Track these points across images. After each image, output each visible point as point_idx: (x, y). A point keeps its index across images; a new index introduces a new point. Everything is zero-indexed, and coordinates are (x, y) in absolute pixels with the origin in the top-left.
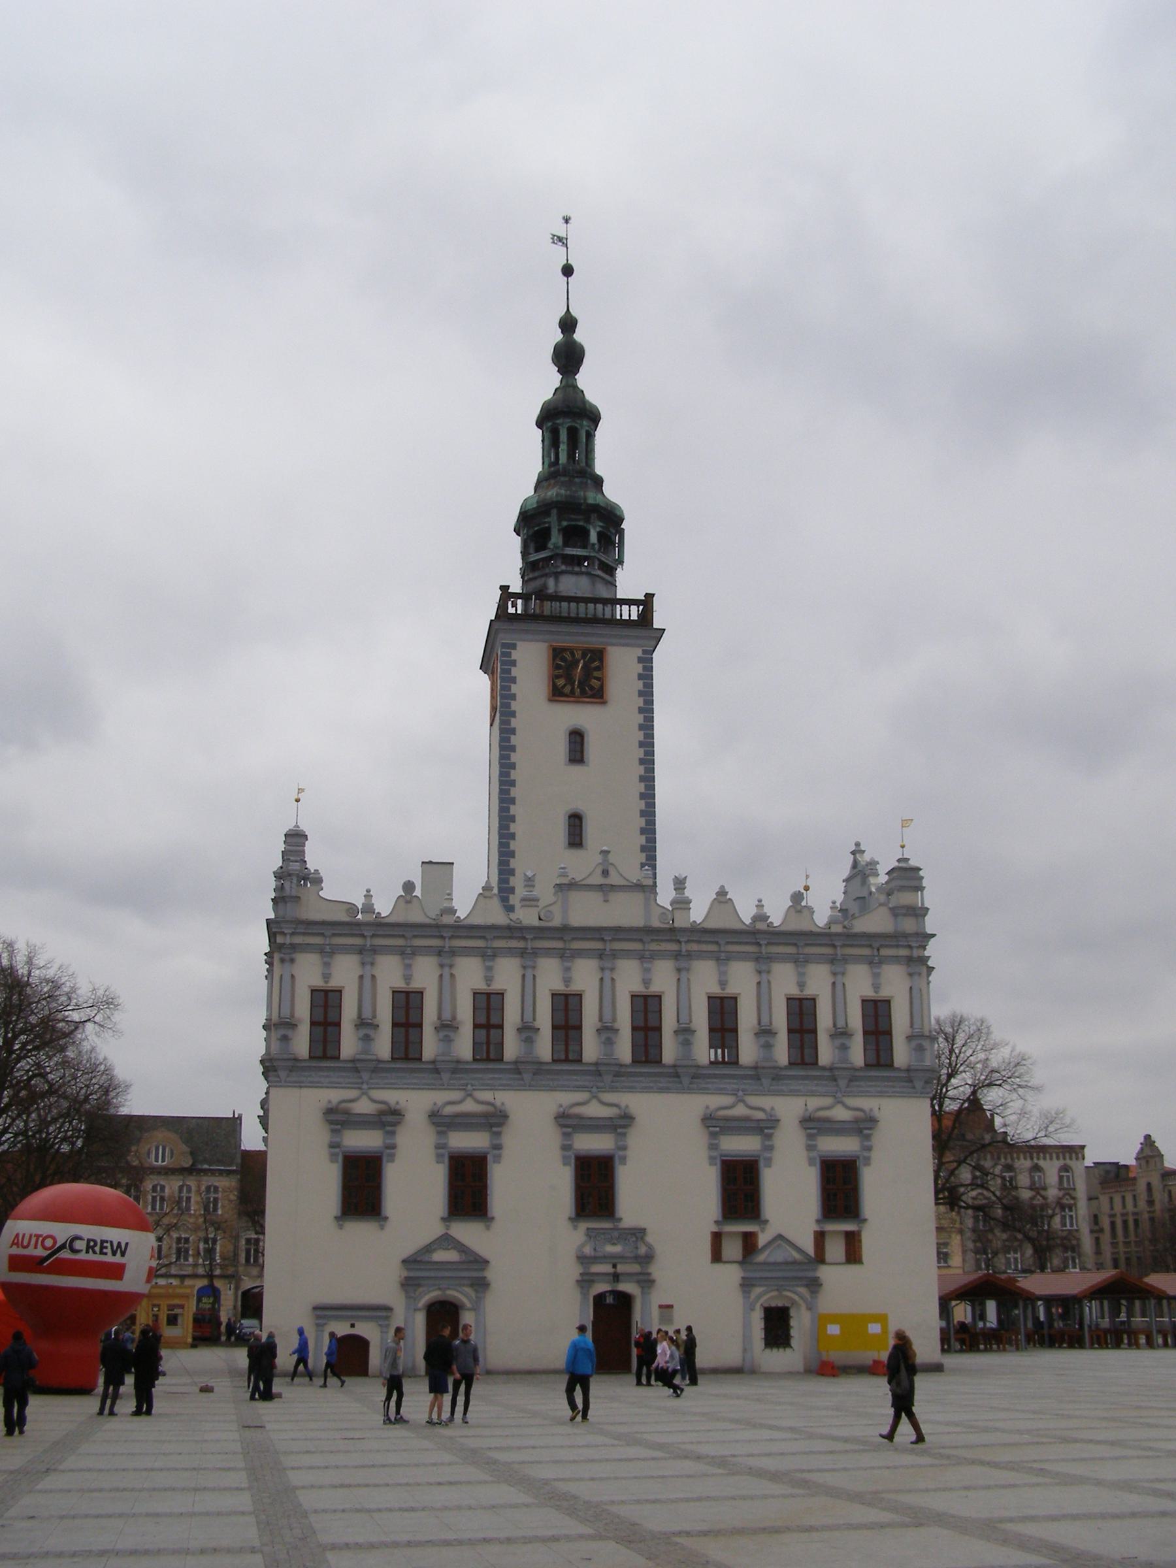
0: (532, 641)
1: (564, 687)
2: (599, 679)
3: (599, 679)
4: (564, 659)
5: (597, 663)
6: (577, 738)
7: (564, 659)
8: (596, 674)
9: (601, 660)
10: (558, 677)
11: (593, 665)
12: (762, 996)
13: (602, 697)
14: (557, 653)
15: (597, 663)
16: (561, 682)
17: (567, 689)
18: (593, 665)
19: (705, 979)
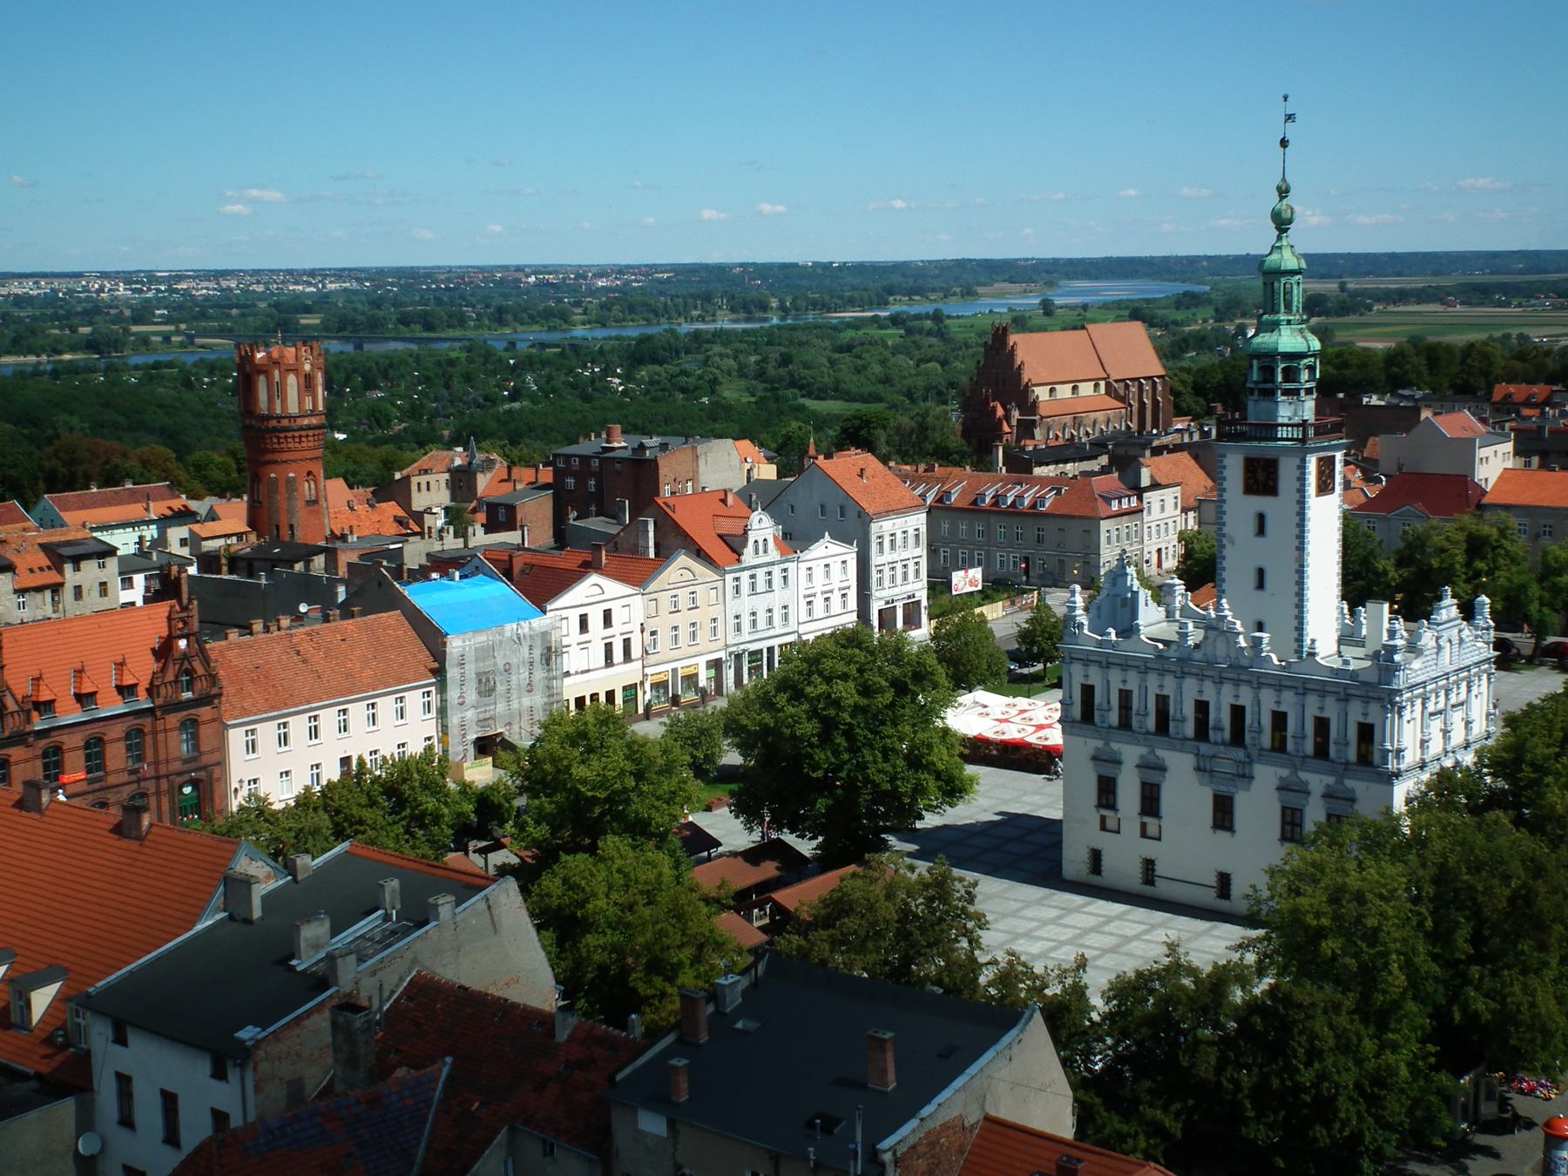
6: (1261, 518)
12: (1302, 716)
19: (1268, 700)
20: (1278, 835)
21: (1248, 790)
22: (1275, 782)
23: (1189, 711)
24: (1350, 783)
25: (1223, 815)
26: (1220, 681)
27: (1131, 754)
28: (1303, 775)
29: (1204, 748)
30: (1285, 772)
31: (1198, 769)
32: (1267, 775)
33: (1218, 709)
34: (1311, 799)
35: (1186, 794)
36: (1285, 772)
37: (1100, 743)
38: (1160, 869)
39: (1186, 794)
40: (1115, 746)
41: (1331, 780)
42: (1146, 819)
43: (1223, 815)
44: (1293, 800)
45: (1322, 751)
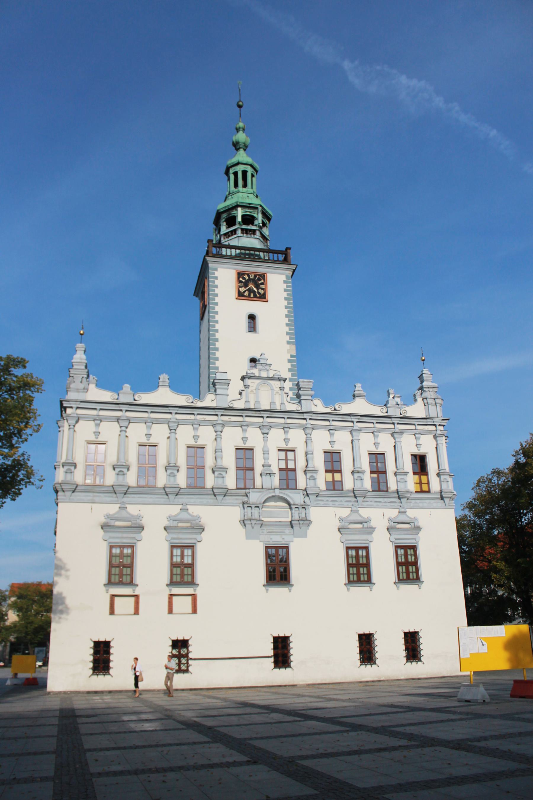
0: (227, 268)
1: (244, 292)
2: (263, 289)
3: (263, 289)
4: (244, 278)
5: (262, 281)
7: (244, 278)
8: (262, 286)
9: (264, 280)
10: (240, 287)
11: (260, 282)
13: (265, 298)
14: (240, 275)
15: (262, 281)
16: (242, 290)
17: (246, 294)
18: (260, 282)
20: (344, 579)
21: (305, 536)
22: (338, 524)
23: (229, 460)
24: (411, 513)
25: (278, 572)
26: (265, 430)
27: (155, 516)
28: (365, 513)
29: (254, 497)
30: (345, 512)
31: (243, 522)
32: (325, 518)
33: (266, 452)
34: (375, 535)
35: (229, 552)
36: (345, 512)
37: (113, 509)
38: (194, 651)
39: (229, 552)
40: (133, 510)
41: (393, 513)
42: (176, 590)
43: (278, 572)
44: (357, 540)
45: (380, 485)
